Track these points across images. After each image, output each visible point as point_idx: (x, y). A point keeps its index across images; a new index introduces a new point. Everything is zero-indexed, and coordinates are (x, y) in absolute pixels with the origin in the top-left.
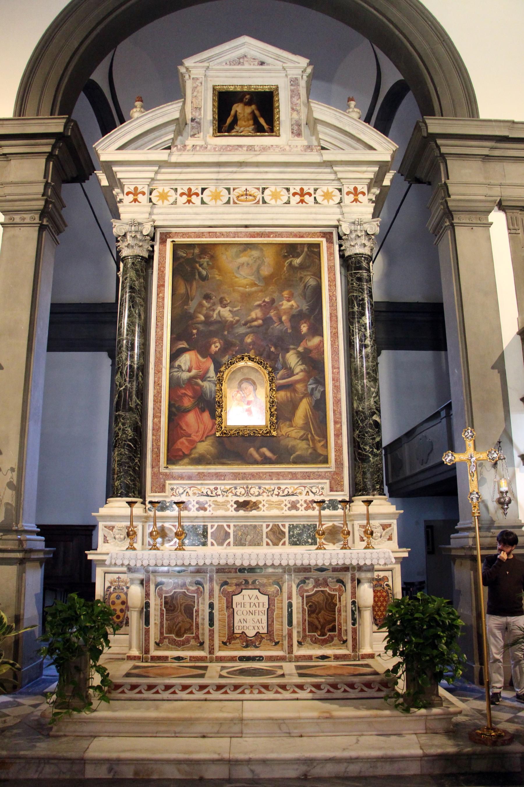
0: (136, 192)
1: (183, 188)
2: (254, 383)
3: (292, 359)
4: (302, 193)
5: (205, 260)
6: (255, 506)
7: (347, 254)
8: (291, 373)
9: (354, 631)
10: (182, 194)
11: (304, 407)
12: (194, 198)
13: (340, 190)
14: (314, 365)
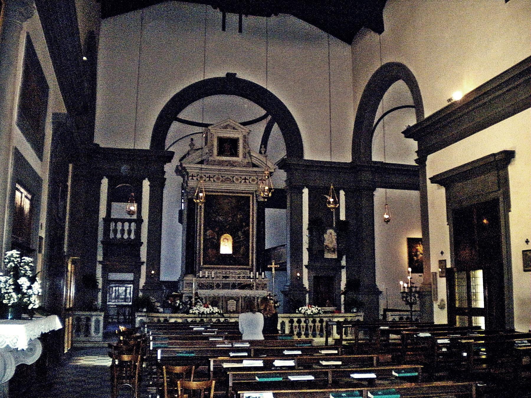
0: (193, 176)
1: (207, 175)
2: (227, 240)
4: (245, 179)
6: (228, 277)
8: (240, 238)
14: (247, 234)
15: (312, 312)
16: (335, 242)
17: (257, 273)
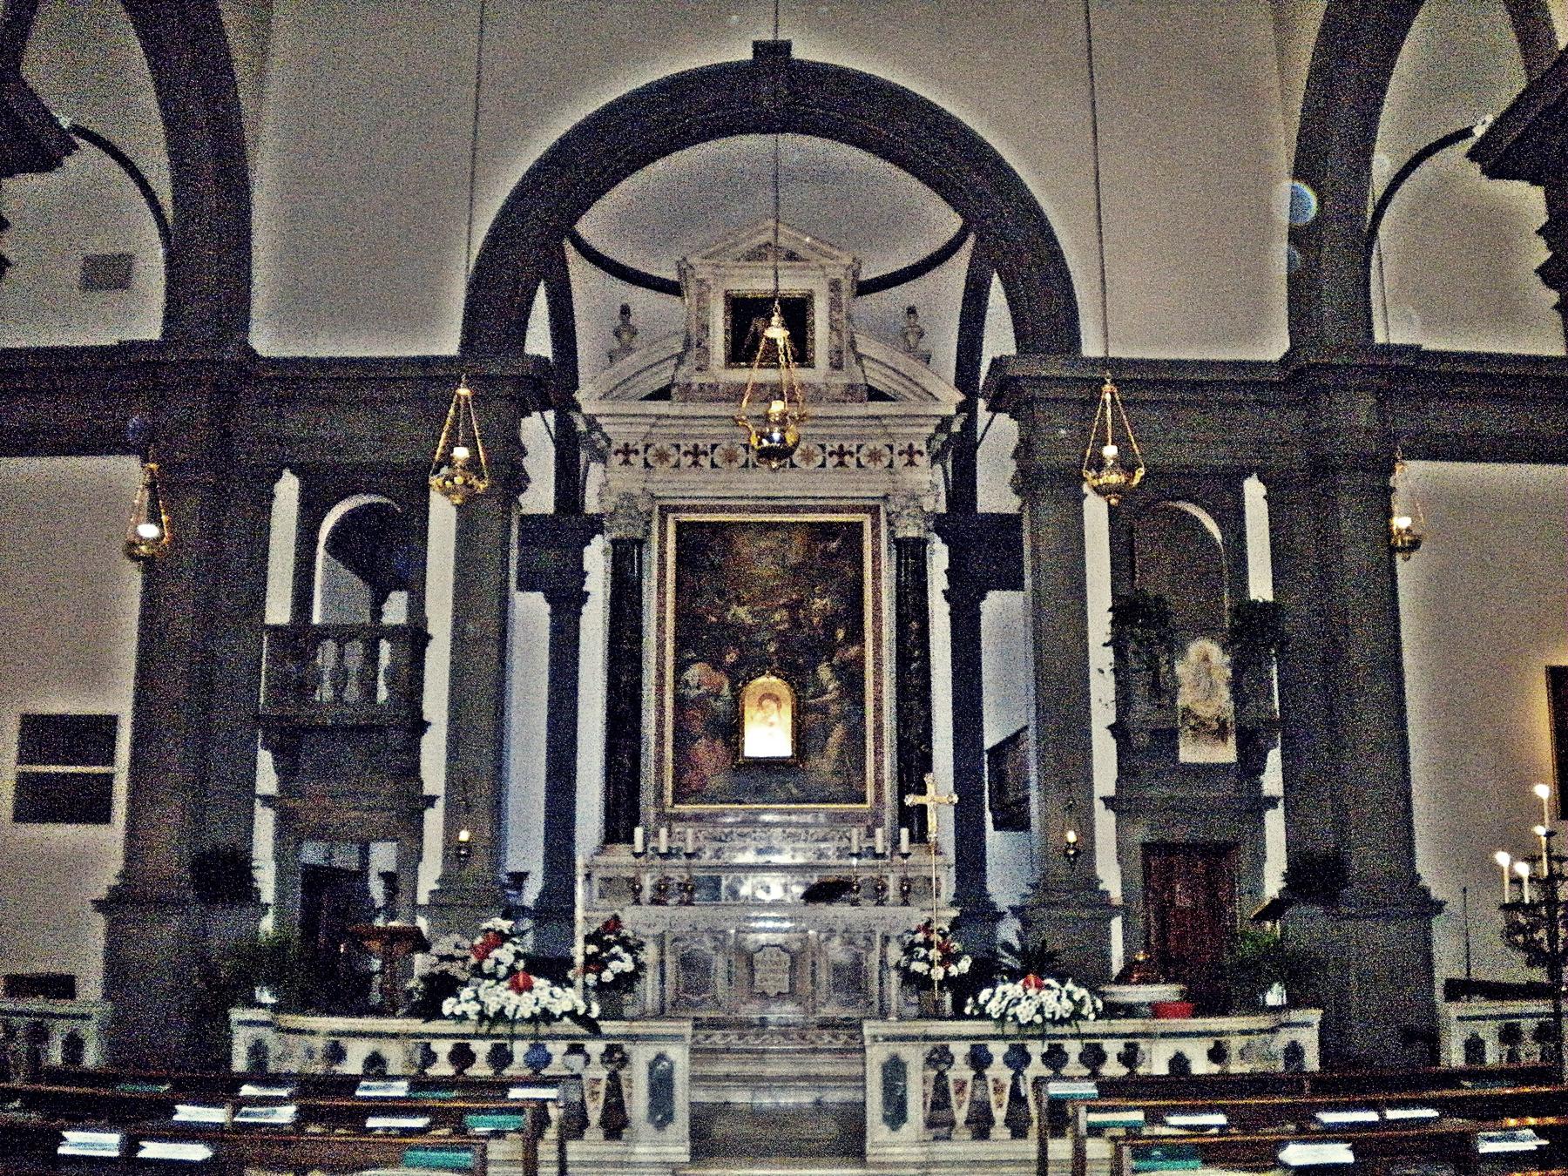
0: (627, 451)
3: (824, 672)
4: (841, 453)
5: (717, 544)
7: (899, 535)
9: (881, 992)
10: (686, 454)
11: (838, 732)
12: (703, 460)
13: (891, 448)
15: (1040, 1010)
16: (1225, 693)
17: (905, 832)
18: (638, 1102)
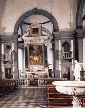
3: (40, 56)
11: (41, 60)
14: (42, 56)
18: (25, 83)
